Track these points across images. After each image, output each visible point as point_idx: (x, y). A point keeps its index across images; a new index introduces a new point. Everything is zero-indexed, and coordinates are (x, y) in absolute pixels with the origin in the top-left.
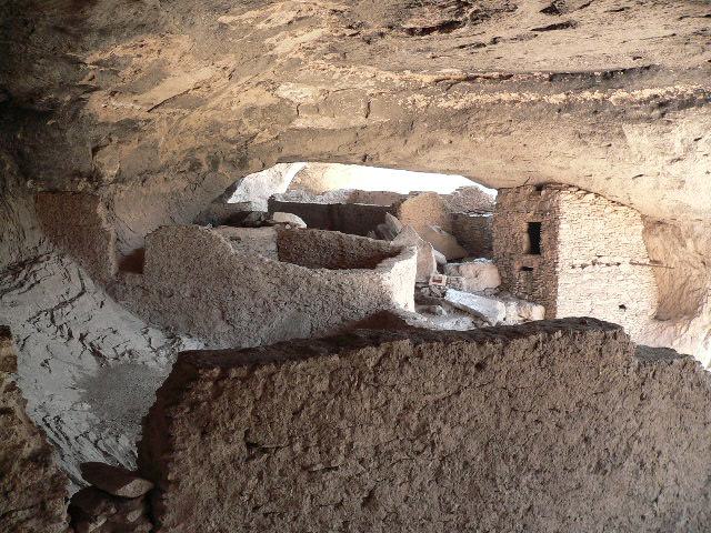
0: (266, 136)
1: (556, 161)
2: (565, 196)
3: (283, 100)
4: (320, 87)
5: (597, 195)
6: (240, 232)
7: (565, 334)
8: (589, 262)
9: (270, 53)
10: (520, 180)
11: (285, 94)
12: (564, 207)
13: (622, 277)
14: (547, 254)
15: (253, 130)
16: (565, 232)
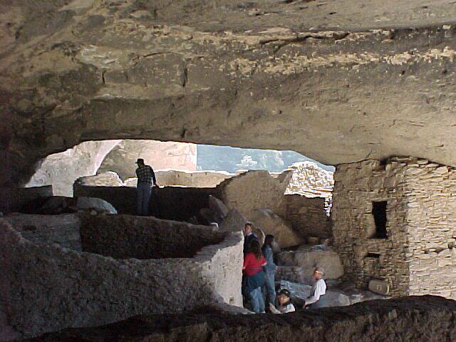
0: (66, 108)
1: (400, 131)
2: (412, 170)
3: (85, 66)
4: (128, 51)
5: (450, 168)
6: (35, 219)
7: (402, 314)
8: (446, 246)
9: (65, 8)
10: (361, 154)
11: (87, 60)
12: (413, 183)
14: (395, 237)
15: (51, 100)
16: (414, 210)
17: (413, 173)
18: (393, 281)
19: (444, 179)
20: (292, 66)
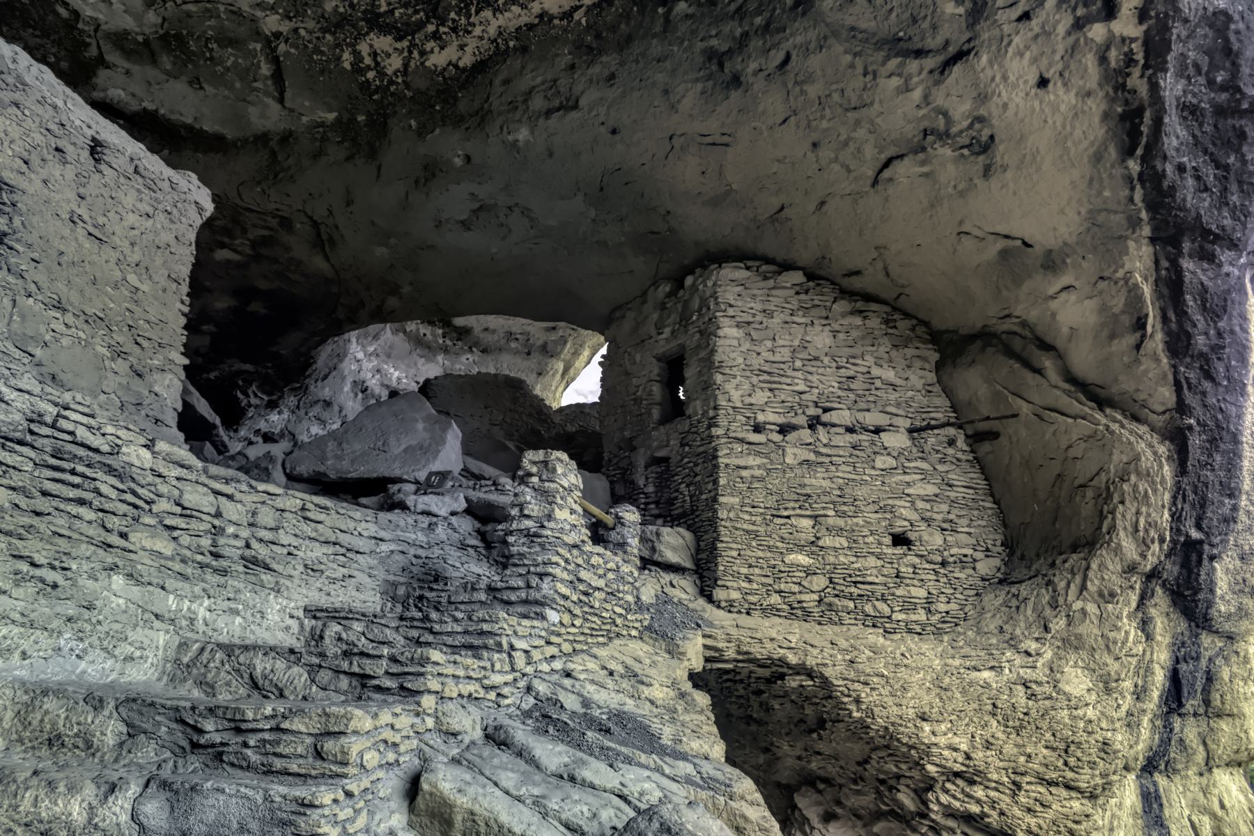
2: (731, 272)
8: (801, 420)
12: (729, 294)
13: (891, 462)
17: (731, 276)
18: (691, 497)
19: (797, 293)
20: (472, 44)
